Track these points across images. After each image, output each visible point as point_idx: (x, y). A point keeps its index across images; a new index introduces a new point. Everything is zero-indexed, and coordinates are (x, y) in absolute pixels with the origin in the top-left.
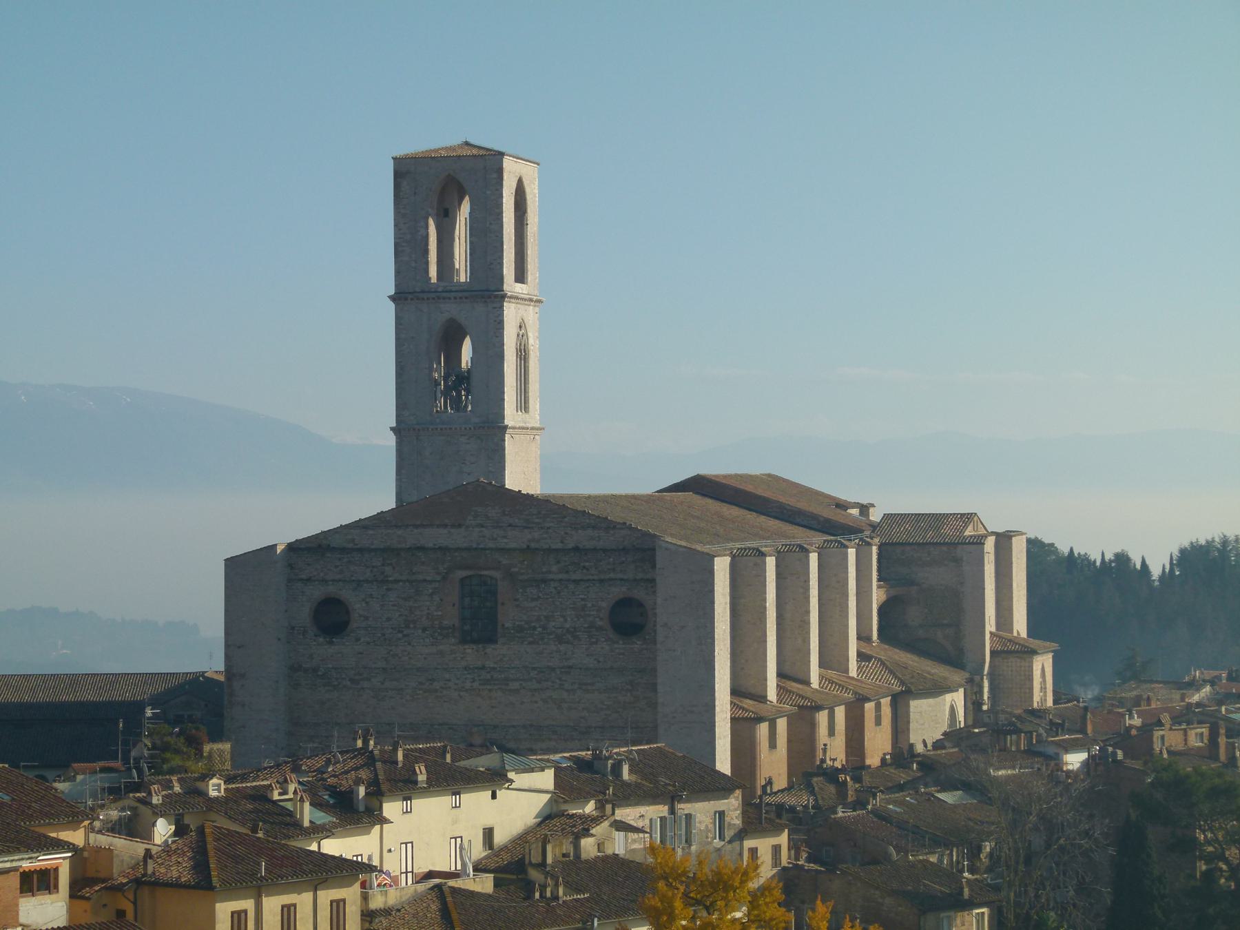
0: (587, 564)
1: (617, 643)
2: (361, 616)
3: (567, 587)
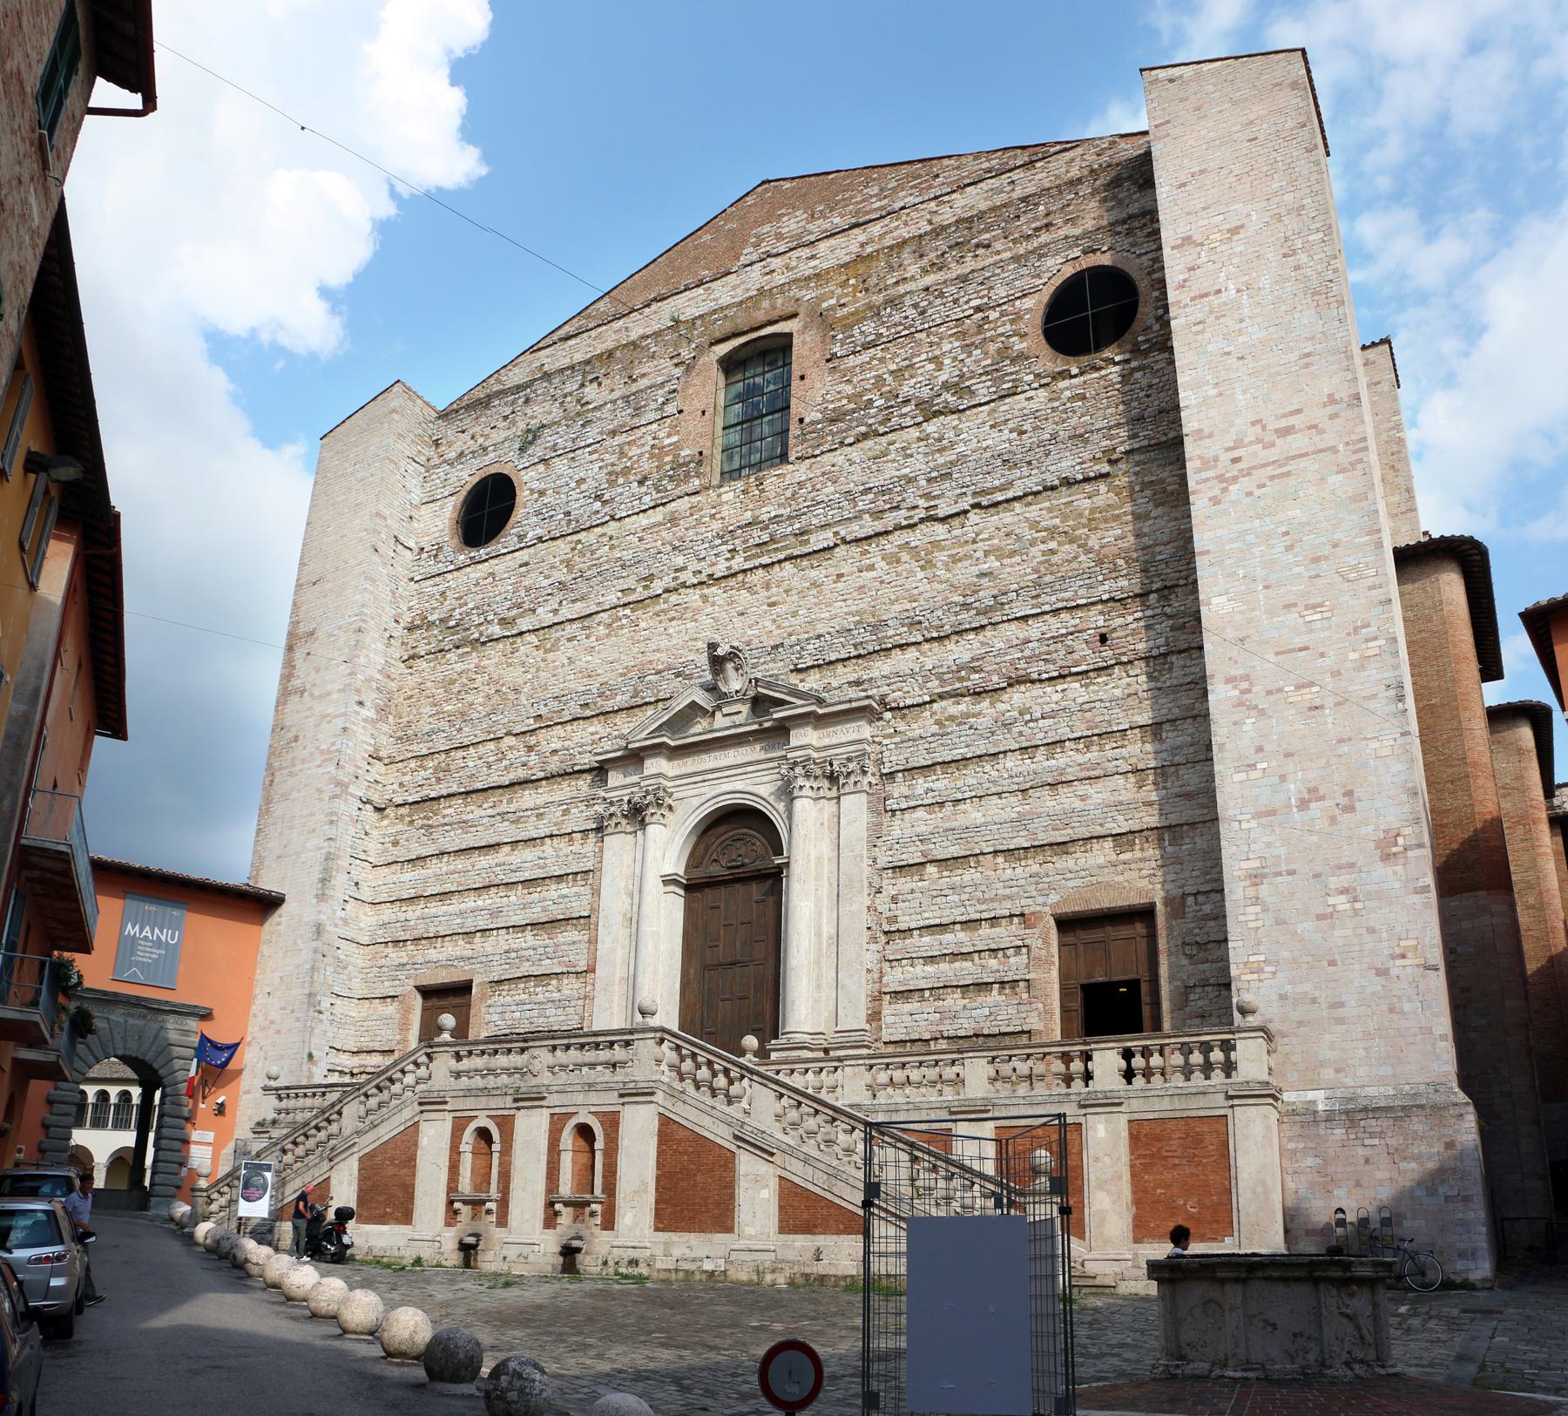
0: (987, 236)
1: (1069, 375)
2: (532, 491)
3: (942, 295)
